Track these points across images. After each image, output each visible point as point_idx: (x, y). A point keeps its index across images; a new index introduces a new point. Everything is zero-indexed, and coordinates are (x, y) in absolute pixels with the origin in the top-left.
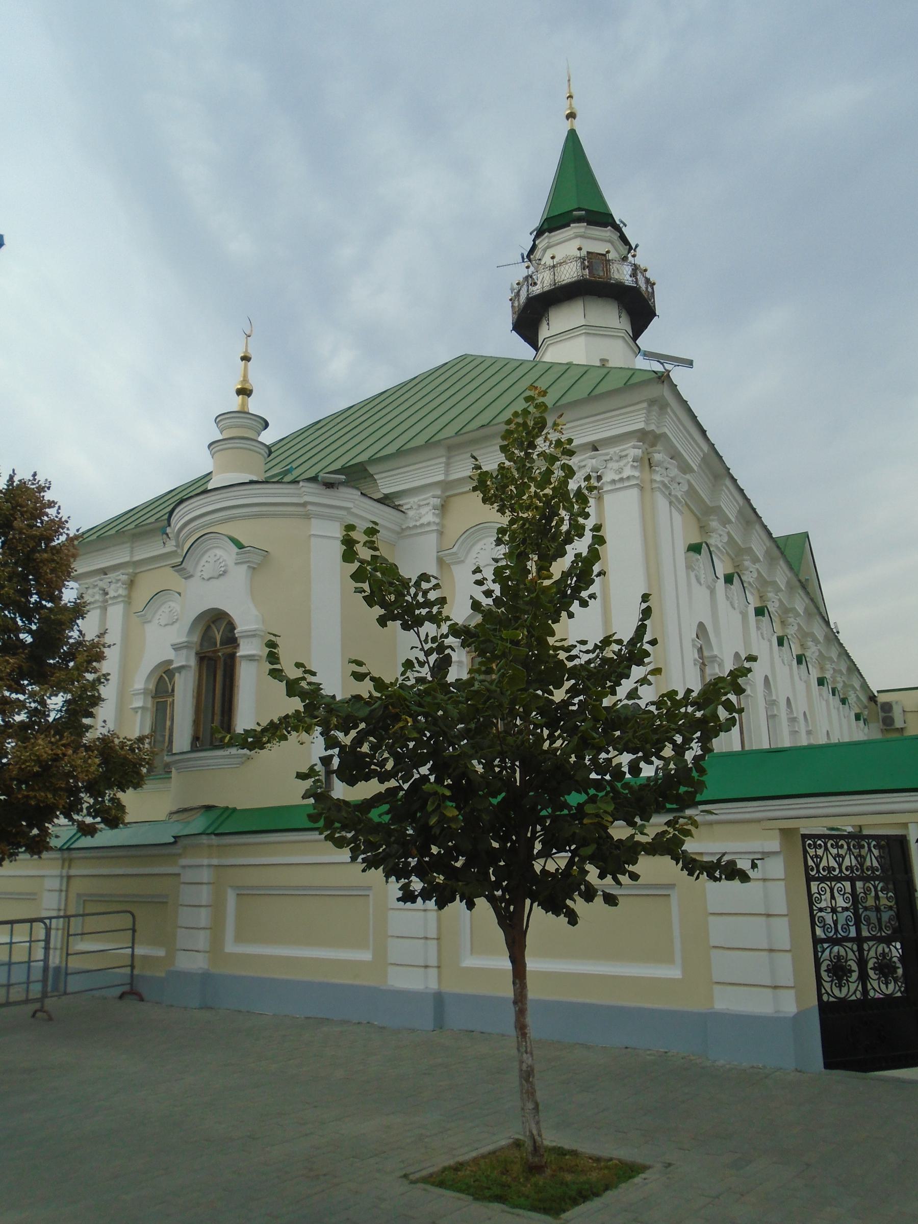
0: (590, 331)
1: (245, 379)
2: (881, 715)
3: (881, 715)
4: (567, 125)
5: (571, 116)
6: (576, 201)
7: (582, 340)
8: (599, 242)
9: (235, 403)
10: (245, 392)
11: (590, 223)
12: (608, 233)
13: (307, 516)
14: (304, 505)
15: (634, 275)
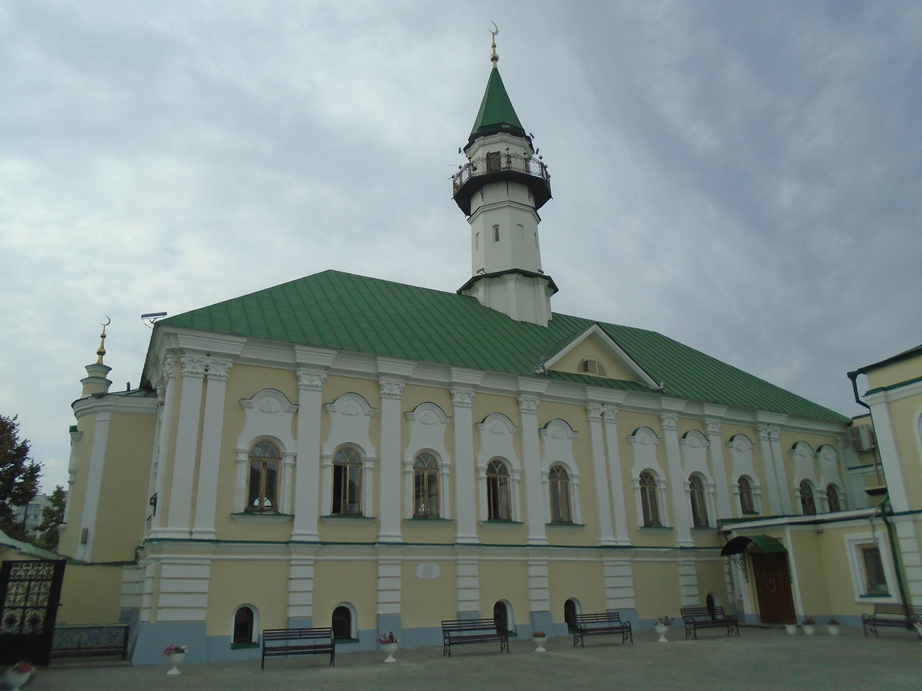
0: (486, 209)
1: (102, 347)
2: (851, 439)
3: (851, 439)
4: (491, 65)
5: (495, 59)
6: (497, 117)
7: (482, 215)
8: (499, 144)
9: (95, 359)
10: (101, 353)
11: (486, 134)
12: (499, 136)
13: (96, 412)
14: (93, 407)
15: (509, 162)
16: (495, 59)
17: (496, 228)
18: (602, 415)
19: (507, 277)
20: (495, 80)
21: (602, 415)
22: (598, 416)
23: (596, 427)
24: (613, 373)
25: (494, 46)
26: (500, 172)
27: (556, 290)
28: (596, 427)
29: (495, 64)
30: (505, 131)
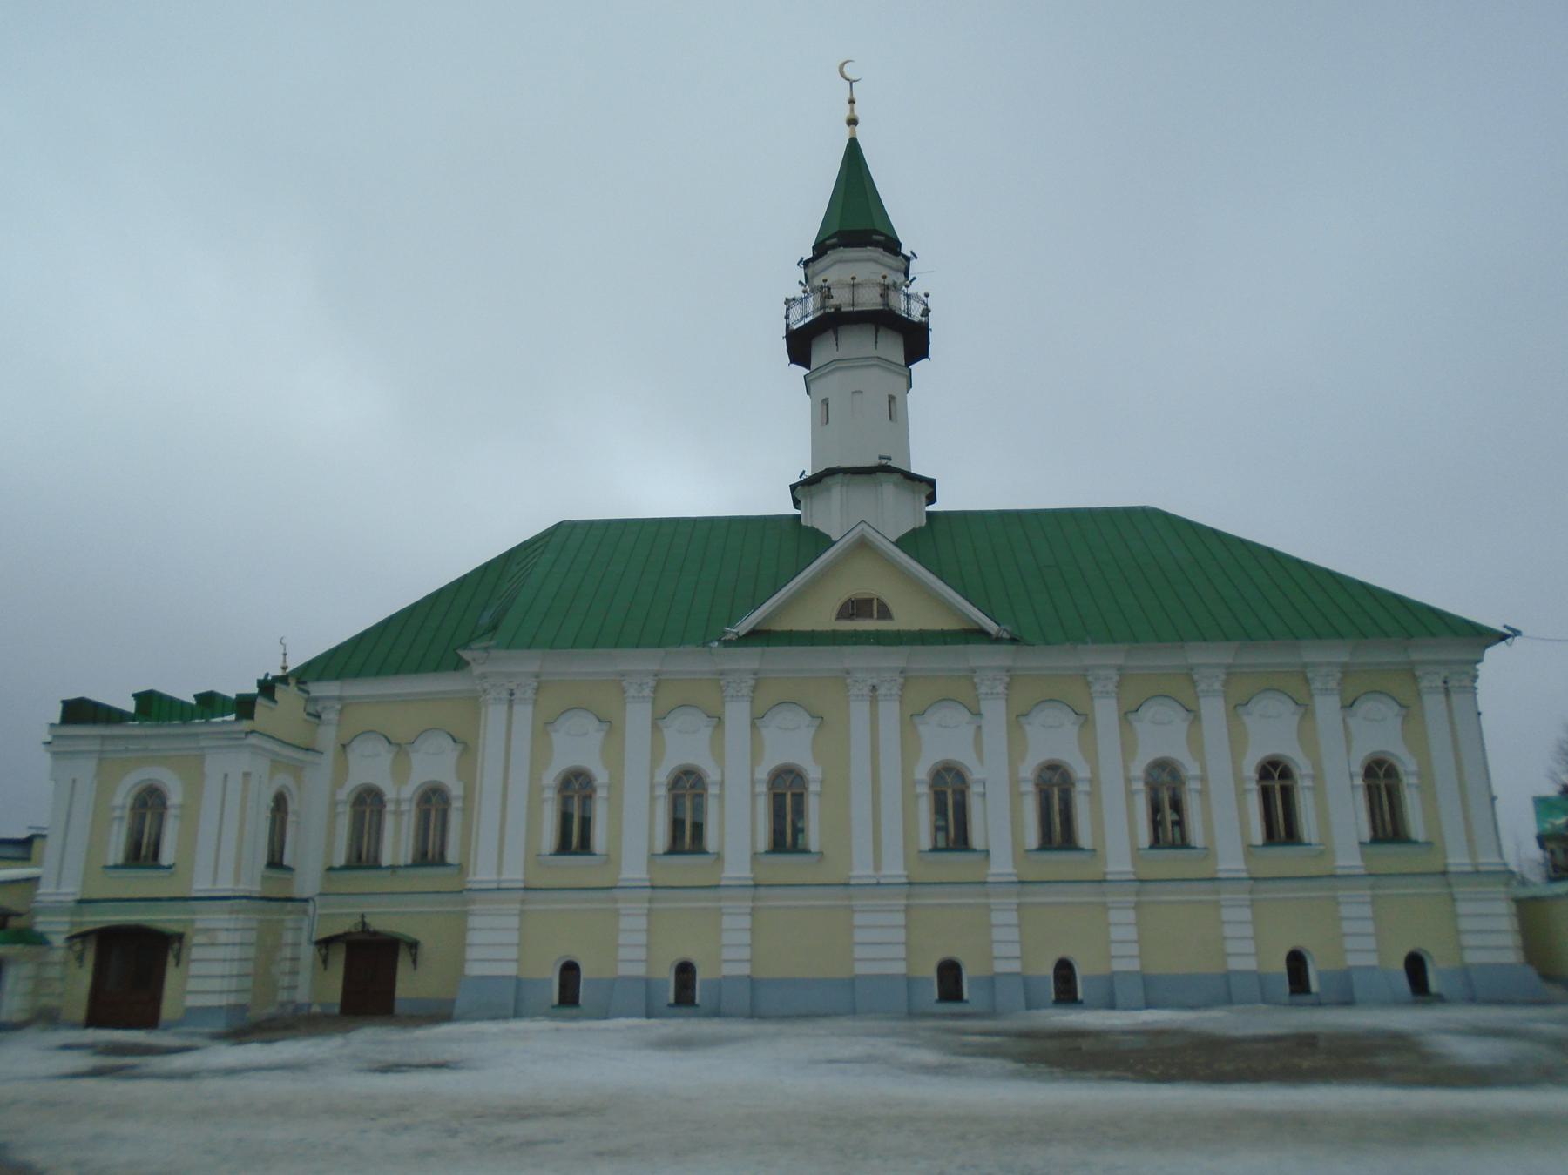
5: (853, 122)
6: (857, 218)
16: (853, 122)
17: (826, 402)
18: (874, 688)
19: (828, 481)
20: (854, 157)
21: (874, 688)
22: (866, 691)
23: (859, 711)
24: (905, 618)
25: (852, 102)
26: (858, 305)
27: (931, 483)
28: (859, 711)
29: (853, 131)
30: (833, 247)
